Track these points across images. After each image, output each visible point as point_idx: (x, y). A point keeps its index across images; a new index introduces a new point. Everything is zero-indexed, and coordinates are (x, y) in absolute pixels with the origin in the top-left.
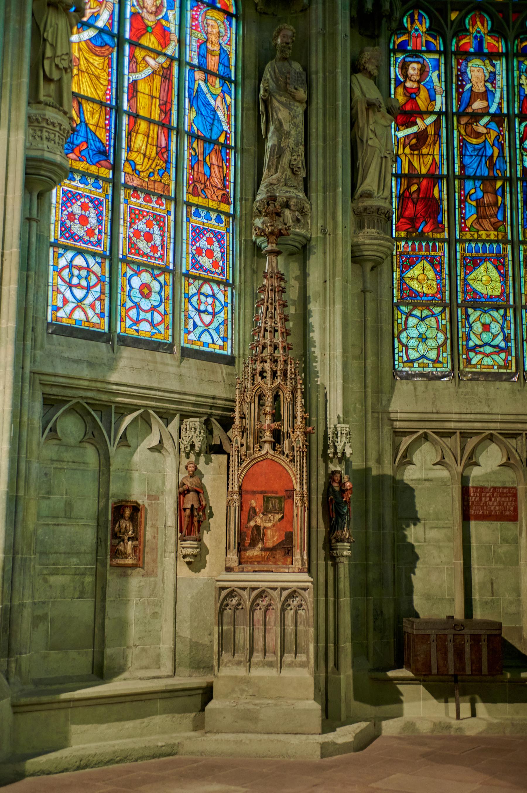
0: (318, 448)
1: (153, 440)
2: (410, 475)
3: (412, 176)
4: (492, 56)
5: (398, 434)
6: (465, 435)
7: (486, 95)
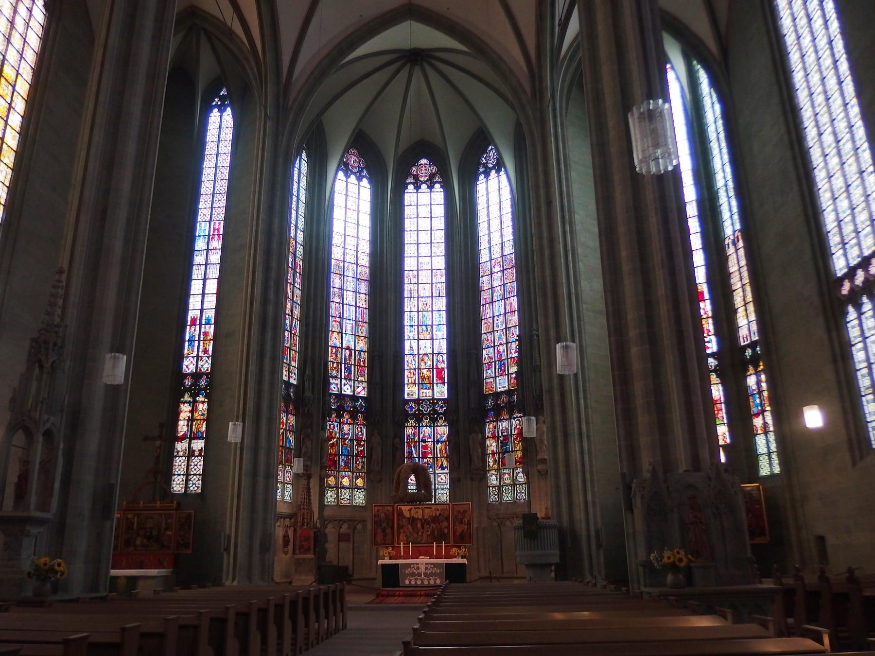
0: (315, 527)
1: (278, 524)
2: (327, 530)
3: (331, 454)
4: (350, 424)
5: (325, 520)
6: (340, 521)
7: (348, 434)
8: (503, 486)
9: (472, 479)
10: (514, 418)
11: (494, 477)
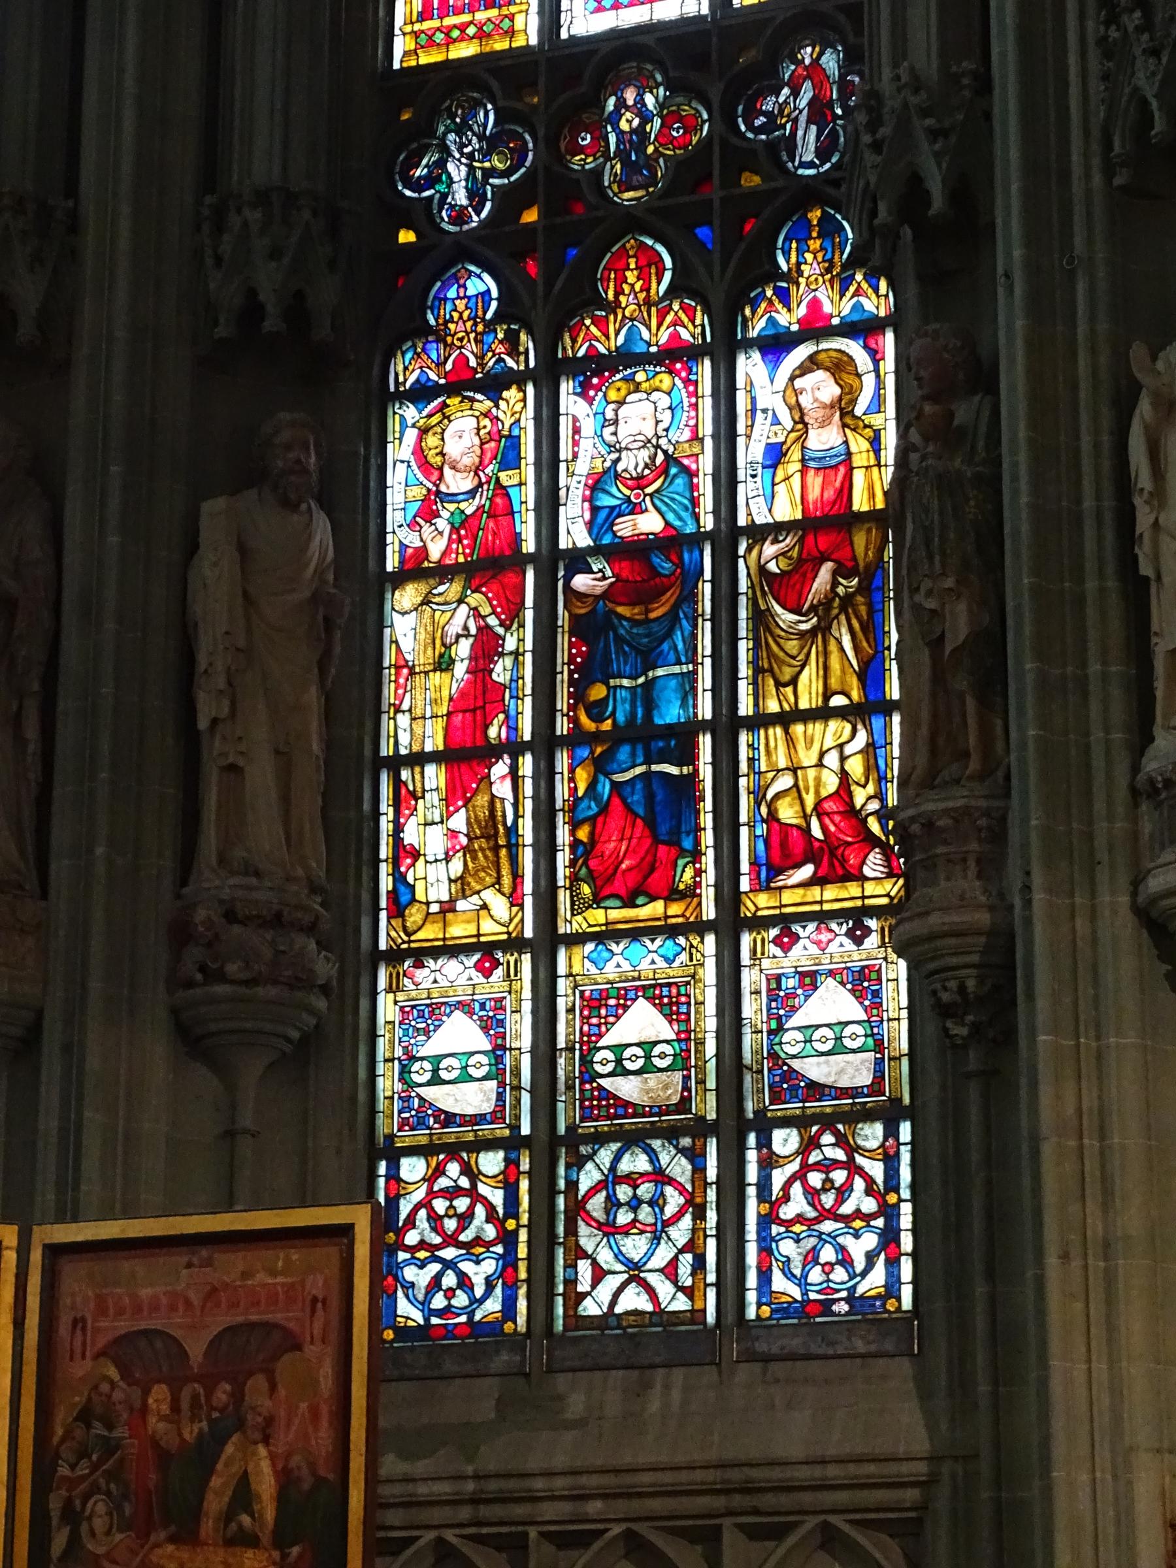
8: (578, 1148)
9: (194, 1041)
10: (775, 346)
11: (460, 1035)
